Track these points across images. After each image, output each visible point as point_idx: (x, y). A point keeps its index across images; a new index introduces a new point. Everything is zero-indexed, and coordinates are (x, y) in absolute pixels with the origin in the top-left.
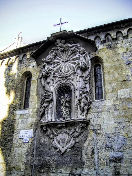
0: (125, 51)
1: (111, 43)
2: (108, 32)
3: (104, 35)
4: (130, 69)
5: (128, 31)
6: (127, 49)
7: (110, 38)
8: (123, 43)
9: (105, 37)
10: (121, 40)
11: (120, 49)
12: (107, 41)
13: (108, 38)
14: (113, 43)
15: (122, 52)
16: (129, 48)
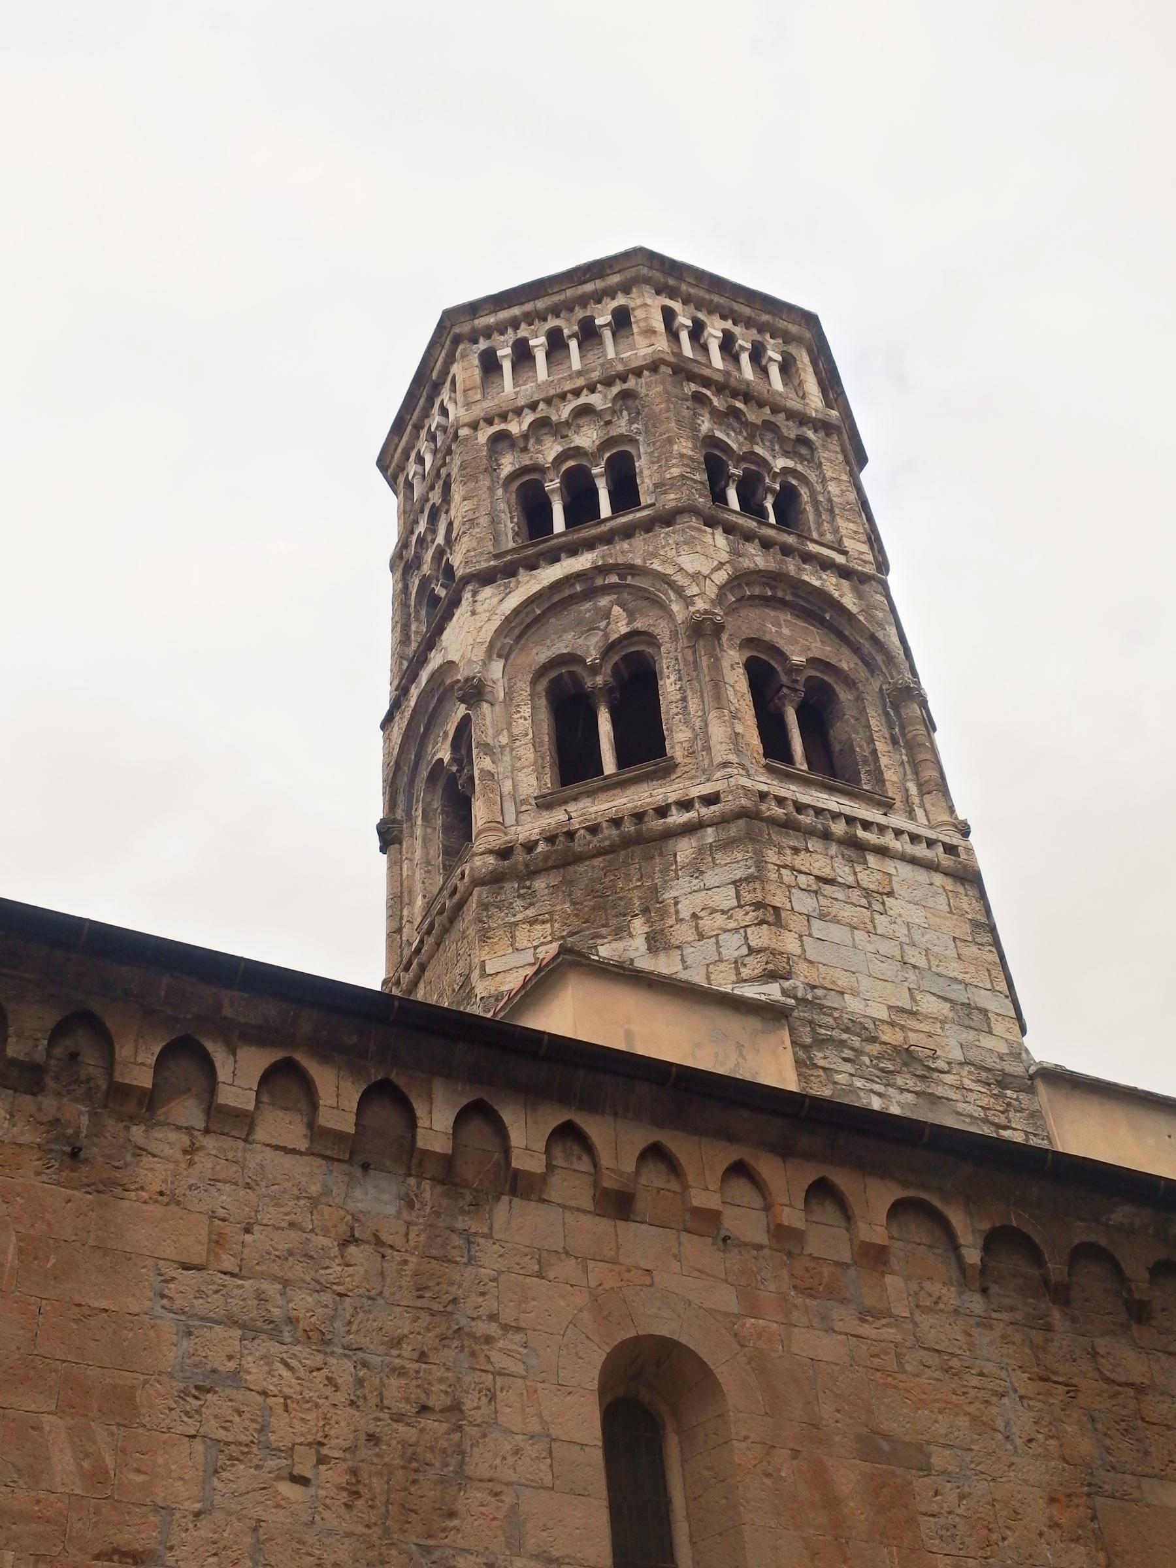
0: (198, 1253)
1: (85, 1120)
2: (95, 1006)
3: (50, 1019)
4: (198, 1446)
5: (267, 1078)
6: (218, 1242)
7: (91, 1063)
8: (191, 1163)
9: (58, 1033)
10: (189, 1130)
11: (155, 1210)
12: (56, 1078)
13: (74, 1056)
14: (112, 1126)
15: (169, 1251)
16: (233, 1231)
